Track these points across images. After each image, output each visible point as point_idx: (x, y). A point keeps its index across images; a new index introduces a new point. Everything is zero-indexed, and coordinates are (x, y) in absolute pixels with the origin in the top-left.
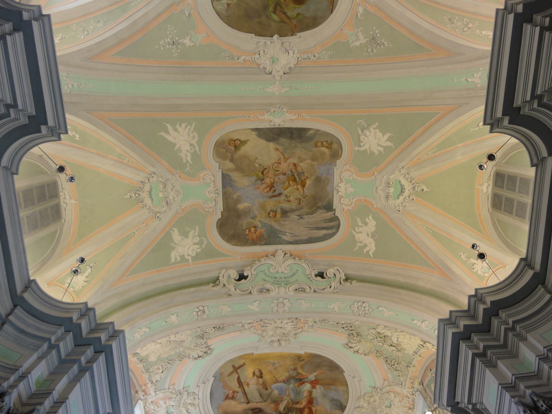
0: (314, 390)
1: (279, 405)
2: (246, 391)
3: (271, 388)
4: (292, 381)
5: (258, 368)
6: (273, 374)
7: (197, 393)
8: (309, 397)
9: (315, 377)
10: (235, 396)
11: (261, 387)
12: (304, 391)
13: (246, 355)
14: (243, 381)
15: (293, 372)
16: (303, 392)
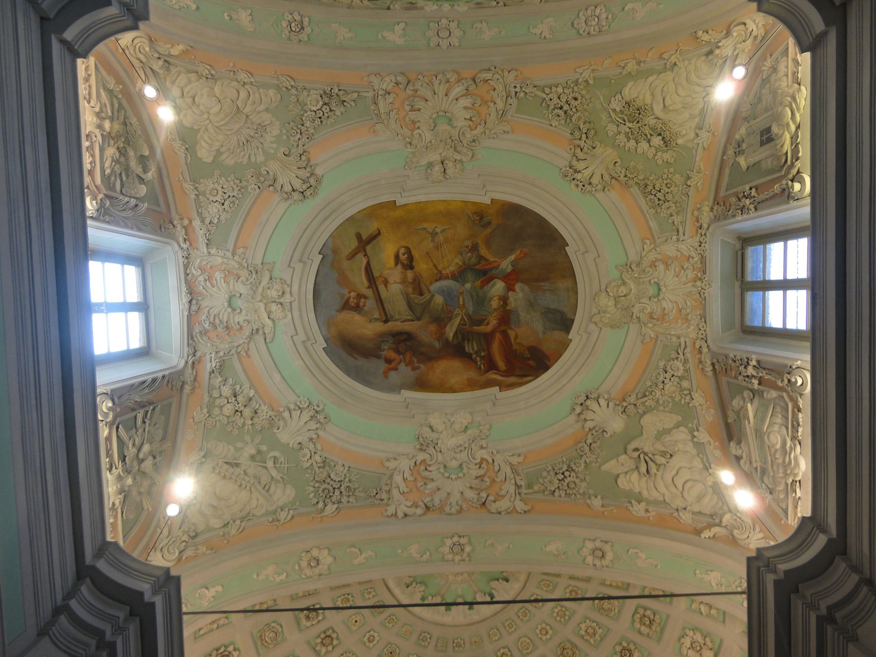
0: (510, 293)
1: (445, 326)
2: (383, 297)
3: (429, 291)
4: (470, 276)
5: (404, 243)
6: (432, 261)
7: (289, 282)
8: (502, 309)
9: (513, 266)
10: (361, 304)
11: (410, 290)
12: (492, 299)
13: (381, 206)
14: (376, 274)
15: (469, 254)
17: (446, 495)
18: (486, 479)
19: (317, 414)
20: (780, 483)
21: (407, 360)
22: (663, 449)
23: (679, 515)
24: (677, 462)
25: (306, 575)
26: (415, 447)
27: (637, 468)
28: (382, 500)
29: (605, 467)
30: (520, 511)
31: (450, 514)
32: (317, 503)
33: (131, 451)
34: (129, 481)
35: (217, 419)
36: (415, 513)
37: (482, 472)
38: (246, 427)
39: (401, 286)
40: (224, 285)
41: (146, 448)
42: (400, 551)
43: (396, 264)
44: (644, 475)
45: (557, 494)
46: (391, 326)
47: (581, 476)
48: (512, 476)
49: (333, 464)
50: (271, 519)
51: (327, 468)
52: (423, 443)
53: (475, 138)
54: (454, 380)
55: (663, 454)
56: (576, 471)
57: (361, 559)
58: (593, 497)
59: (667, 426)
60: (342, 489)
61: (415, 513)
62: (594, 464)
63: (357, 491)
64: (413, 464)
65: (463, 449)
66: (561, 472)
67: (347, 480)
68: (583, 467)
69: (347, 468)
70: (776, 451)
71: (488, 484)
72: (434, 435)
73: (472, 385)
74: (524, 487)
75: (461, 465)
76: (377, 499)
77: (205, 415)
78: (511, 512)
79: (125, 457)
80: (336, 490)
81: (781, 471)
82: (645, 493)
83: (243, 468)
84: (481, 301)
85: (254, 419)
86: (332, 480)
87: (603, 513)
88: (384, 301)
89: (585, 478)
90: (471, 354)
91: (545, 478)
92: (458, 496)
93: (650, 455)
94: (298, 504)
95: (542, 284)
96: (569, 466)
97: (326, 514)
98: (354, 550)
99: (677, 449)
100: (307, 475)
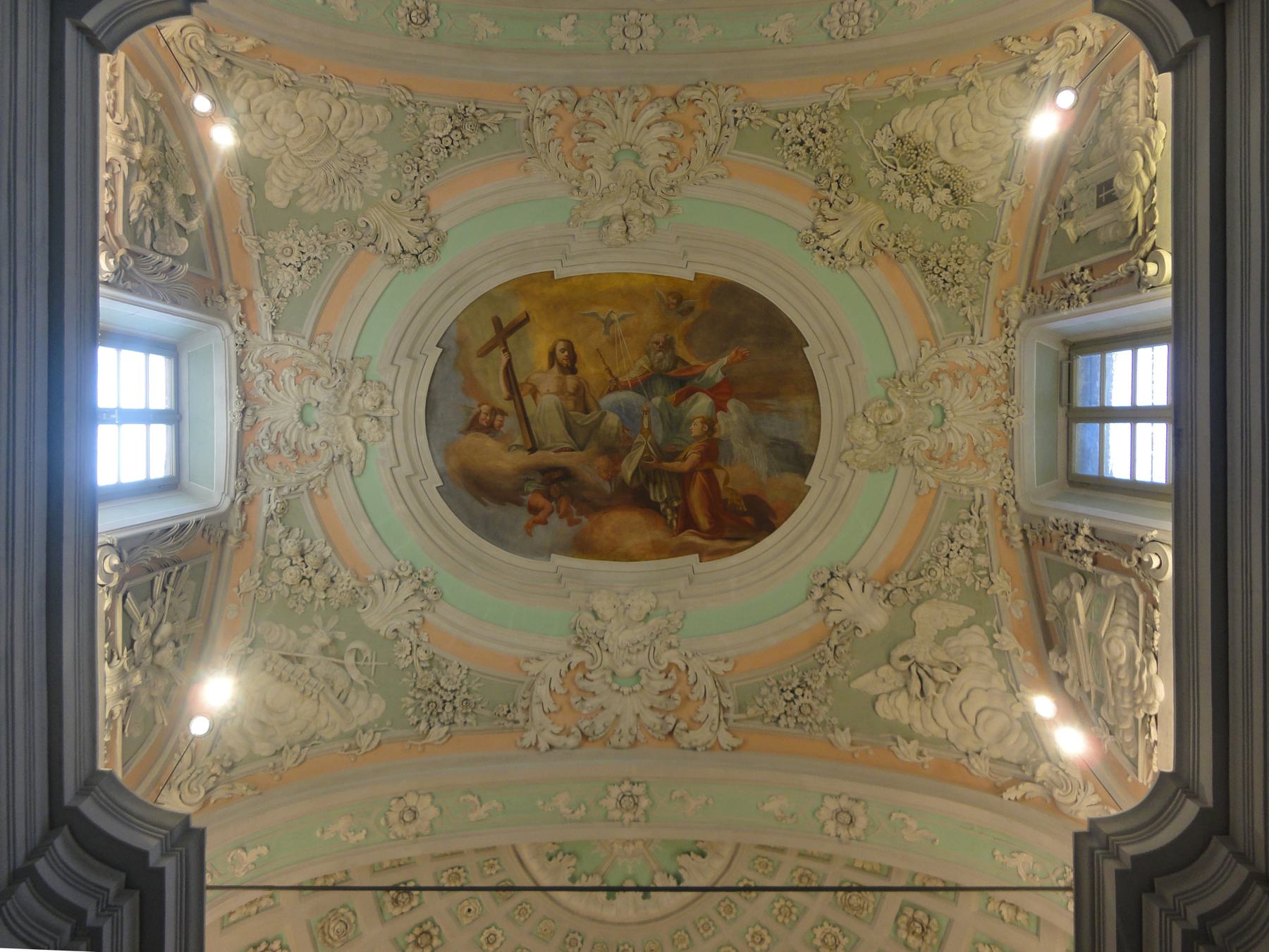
0: (720, 414)
1: (621, 460)
2: (529, 414)
3: (599, 407)
4: (660, 386)
5: (563, 335)
6: (604, 363)
7: (391, 387)
8: (706, 438)
9: (724, 374)
10: (497, 423)
11: (570, 405)
12: (692, 421)
13: (530, 278)
14: (520, 380)
15: (660, 354)
16: (690, 422)
17: (613, 717)
18: (676, 695)
19: (424, 587)
20: (1126, 717)
21: (563, 508)
22: (946, 659)
23: (969, 762)
24: (967, 679)
25: (395, 834)
26: (569, 643)
27: (906, 686)
28: (516, 722)
29: (856, 684)
30: (725, 747)
31: (618, 748)
32: (418, 722)
33: (142, 634)
34: (137, 679)
35: (273, 588)
36: (565, 744)
37: (669, 684)
38: (317, 603)
39: (556, 398)
40: (294, 388)
41: (166, 629)
42: (540, 803)
43: (551, 365)
44: (917, 698)
45: (782, 722)
46: (541, 457)
47: (821, 697)
48: (715, 693)
49: (444, 664)
50: (346, 746)
51: (435, 670)
52: (581, 636)
53: (674, 183)
54: (631, 542)
55: (947, 666)
56: (813, 687)
57: (481, 812)
58: (837, 730)
59: (951, 624)
60: (457, 703)
61: (565, 744)
62: (840, 678)
63: (480, 706)
64: (565, 668)
65: (642, 648)
66: (790, 688)
67: (464, 689)
68: (823, 682)
69: (465, 671)
70: (1120, 667)
71: (678, 703)
72: (599, 625)
73: (659, 551)
74: (732, 710)
75: (638, 672)
76: (508, 721)
77: (256, 583)
78: (712, 749)
79: (133, 641)
80: (447, 704)
81: (1127, 699)
82: (918, 727)
83: (309, 665)
84: (675, 424)
85: (329, 591)
86: (442, 688)
87: (853, 755)
88: (530, 419)
89: (826, 700)
90: (658, 504)
91: (765, 697)
92: (632, 720)
93: (926, 668)
94: (388, 723)
95: (768, 402)
96: (802, 680)
97: (430, 740)
98: (470, 797)
99: (967, 659)
100: (405, 680)
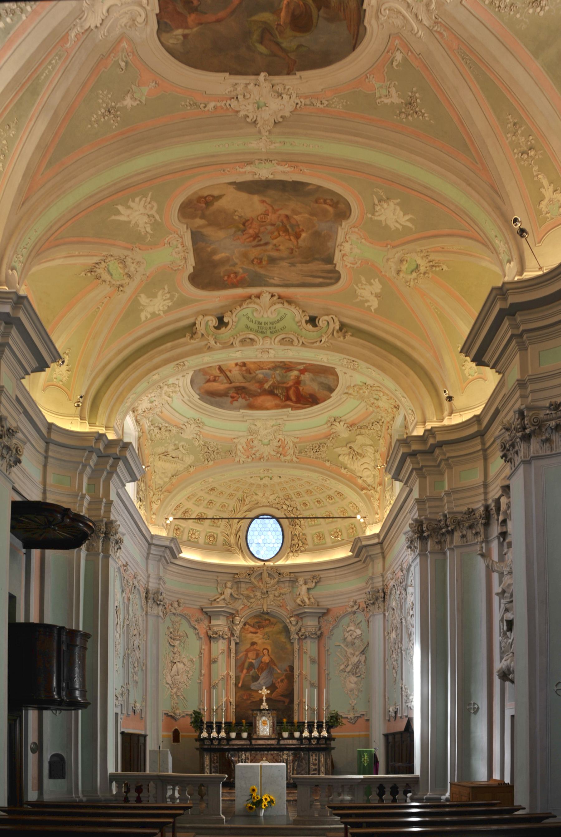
0: (302, 375)
54: (268, 404)
64: (246, 441)
